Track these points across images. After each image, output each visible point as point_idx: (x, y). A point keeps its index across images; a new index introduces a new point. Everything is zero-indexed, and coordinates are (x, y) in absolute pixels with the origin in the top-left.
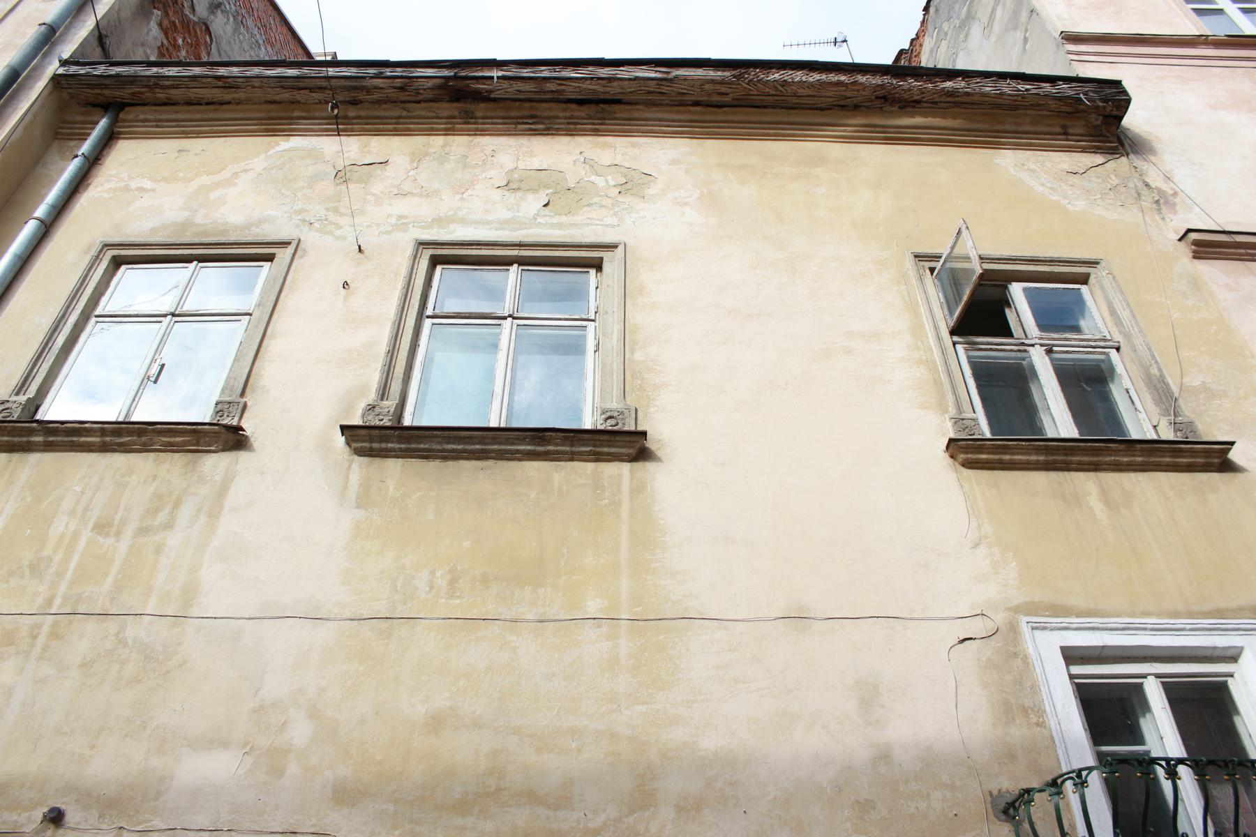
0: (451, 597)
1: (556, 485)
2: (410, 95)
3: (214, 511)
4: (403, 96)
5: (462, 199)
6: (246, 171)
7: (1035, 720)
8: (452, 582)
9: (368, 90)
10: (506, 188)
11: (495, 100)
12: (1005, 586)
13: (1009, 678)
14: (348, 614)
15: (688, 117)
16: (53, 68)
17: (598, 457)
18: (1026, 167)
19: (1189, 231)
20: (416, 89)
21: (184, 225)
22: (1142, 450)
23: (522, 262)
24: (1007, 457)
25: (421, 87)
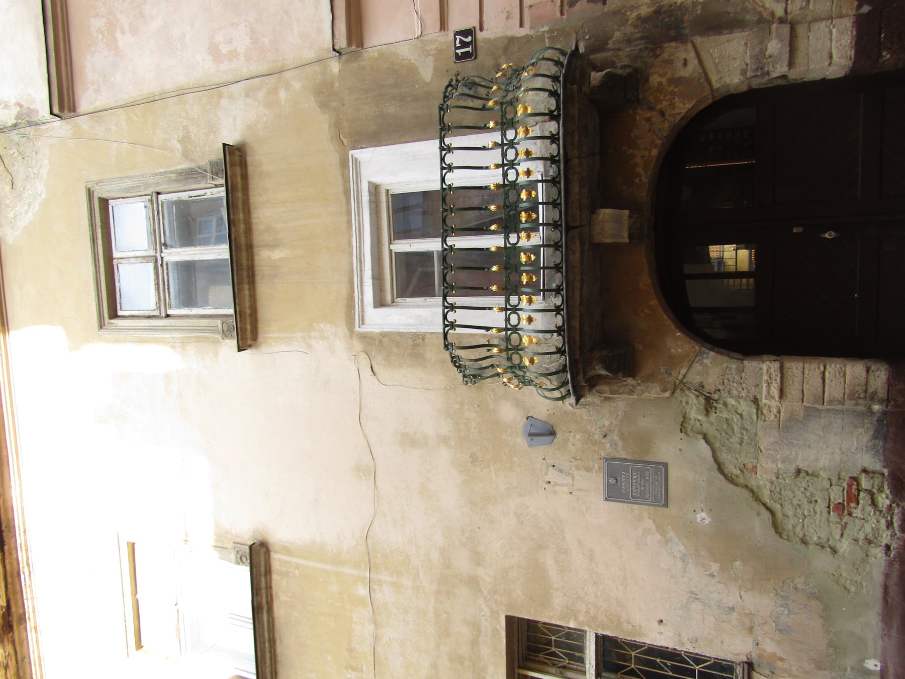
0: (361, 670)
1: (288, 599)
2: (11, 660)
4: (12, 664)
7: (421, 341)
8: (354, 669)
11: (8, 601)
12: (336, 336)
13: (395, 350)
17: (268, 572)
18: (13, 220)
19: (52, 113)
20: (6, 658)
22: (234, 214)
24: (248, 311)
25: (3, 655)
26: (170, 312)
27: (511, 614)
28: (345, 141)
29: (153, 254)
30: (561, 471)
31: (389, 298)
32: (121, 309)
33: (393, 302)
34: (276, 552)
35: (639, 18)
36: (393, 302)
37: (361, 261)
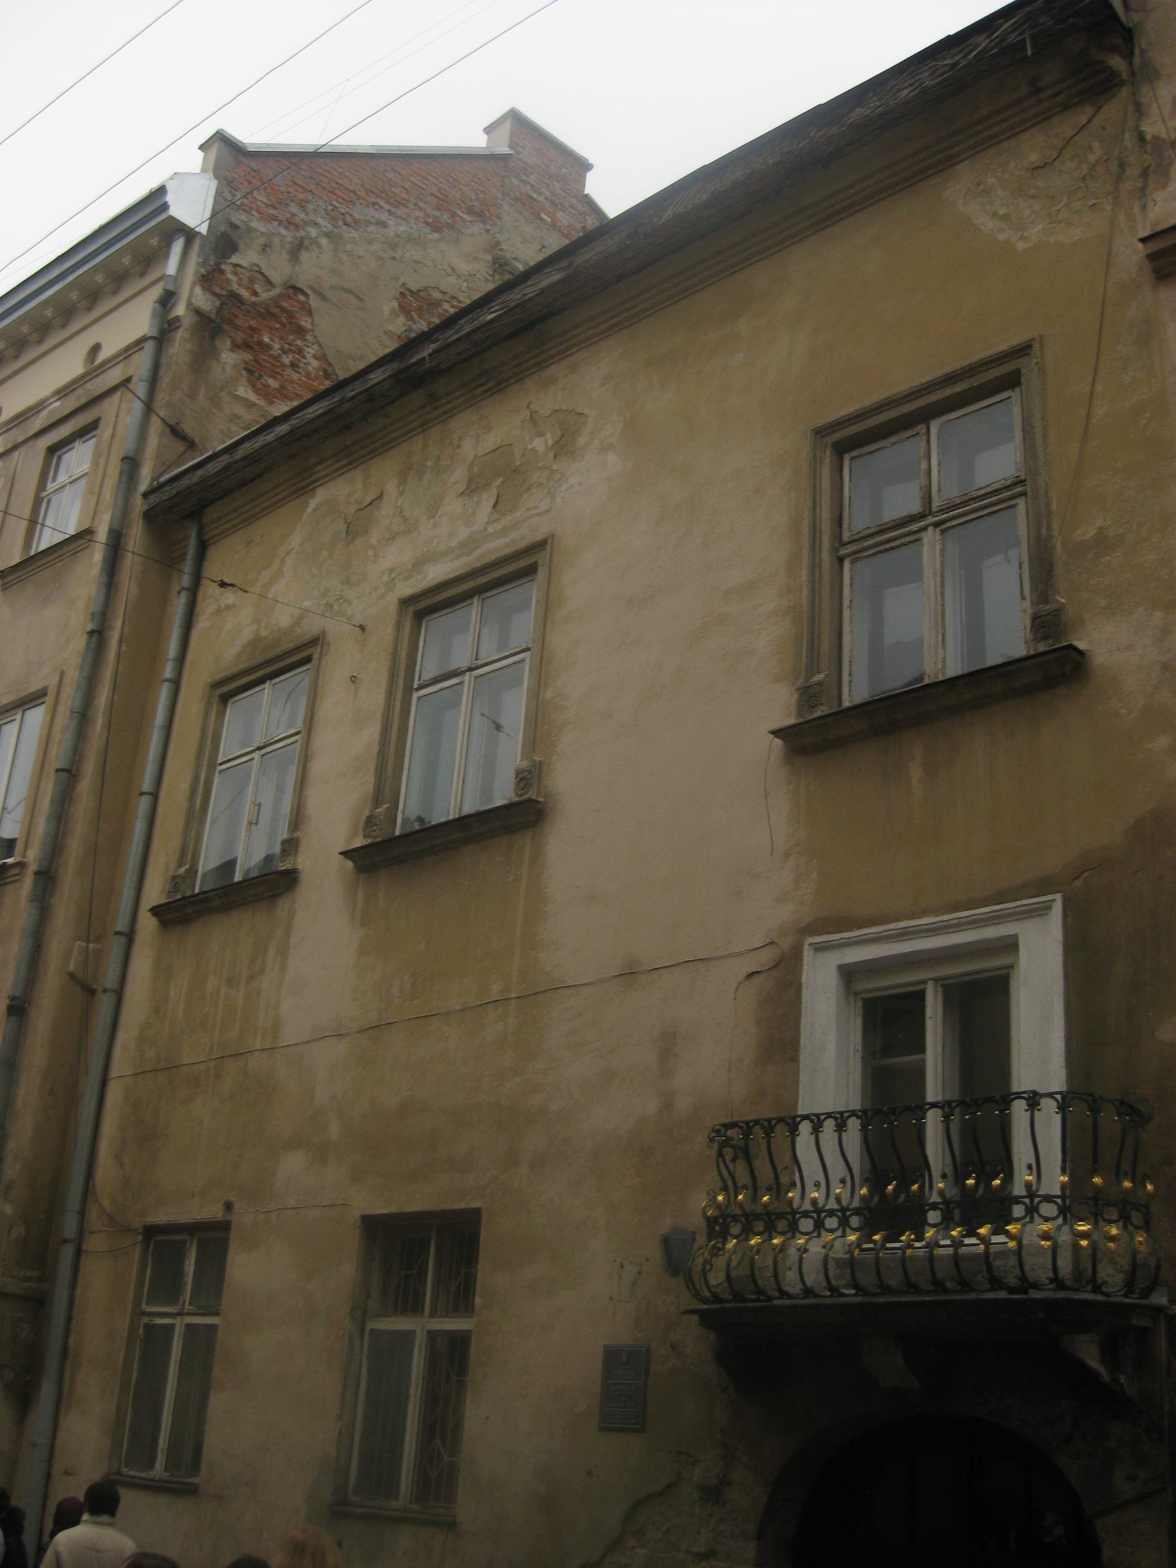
3: (283, 952)
5: (435, 525)
6: (288, 553)
10: (467, 491)
16: (139, 505)
18: (981, 188)
21: (256, 641)
23: (481, 591)
26: (847, 565)
27: (485, 1217)
28: (1078, 883)
29: (934, 509)
30: (634, 1284)
31: (860, 986)
32: (852, 459)
33: (856, 994)
36: (856, 994)
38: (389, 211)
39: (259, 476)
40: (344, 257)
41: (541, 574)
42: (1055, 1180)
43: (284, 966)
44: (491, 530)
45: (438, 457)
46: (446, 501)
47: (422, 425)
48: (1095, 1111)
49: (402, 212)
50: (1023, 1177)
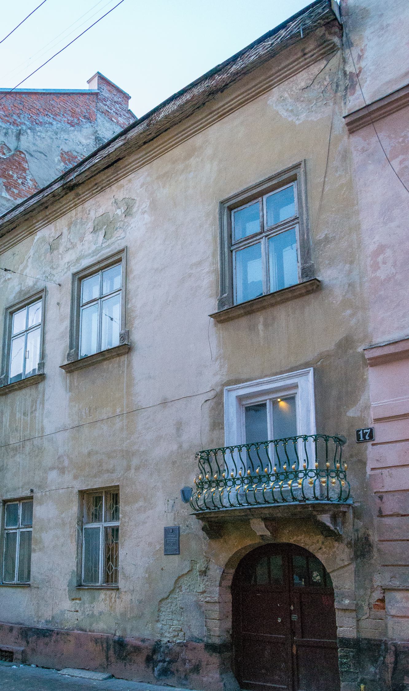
3: (43, 403)
5: (83, 244)
8: (90, 410)
9: (46, 202)
14: (71, 427)
15: (144, 152)
34: (127, 358)
35: (368, 535)
37: (258, 384)
38: (53, 118)
39: (15, 228)
40: (37, 137)
41: (124, 261)
42: (314, 465)
43: (43, 408)
44: (103, 246)
45: (82, 218)
46: (86, 235)
47: (74, 206)
48: (326, 440)
49: (58, 118)
50: (302, 464)
